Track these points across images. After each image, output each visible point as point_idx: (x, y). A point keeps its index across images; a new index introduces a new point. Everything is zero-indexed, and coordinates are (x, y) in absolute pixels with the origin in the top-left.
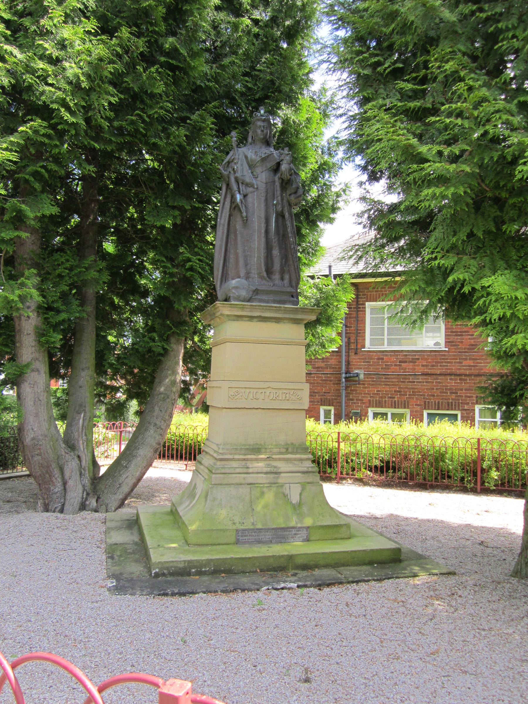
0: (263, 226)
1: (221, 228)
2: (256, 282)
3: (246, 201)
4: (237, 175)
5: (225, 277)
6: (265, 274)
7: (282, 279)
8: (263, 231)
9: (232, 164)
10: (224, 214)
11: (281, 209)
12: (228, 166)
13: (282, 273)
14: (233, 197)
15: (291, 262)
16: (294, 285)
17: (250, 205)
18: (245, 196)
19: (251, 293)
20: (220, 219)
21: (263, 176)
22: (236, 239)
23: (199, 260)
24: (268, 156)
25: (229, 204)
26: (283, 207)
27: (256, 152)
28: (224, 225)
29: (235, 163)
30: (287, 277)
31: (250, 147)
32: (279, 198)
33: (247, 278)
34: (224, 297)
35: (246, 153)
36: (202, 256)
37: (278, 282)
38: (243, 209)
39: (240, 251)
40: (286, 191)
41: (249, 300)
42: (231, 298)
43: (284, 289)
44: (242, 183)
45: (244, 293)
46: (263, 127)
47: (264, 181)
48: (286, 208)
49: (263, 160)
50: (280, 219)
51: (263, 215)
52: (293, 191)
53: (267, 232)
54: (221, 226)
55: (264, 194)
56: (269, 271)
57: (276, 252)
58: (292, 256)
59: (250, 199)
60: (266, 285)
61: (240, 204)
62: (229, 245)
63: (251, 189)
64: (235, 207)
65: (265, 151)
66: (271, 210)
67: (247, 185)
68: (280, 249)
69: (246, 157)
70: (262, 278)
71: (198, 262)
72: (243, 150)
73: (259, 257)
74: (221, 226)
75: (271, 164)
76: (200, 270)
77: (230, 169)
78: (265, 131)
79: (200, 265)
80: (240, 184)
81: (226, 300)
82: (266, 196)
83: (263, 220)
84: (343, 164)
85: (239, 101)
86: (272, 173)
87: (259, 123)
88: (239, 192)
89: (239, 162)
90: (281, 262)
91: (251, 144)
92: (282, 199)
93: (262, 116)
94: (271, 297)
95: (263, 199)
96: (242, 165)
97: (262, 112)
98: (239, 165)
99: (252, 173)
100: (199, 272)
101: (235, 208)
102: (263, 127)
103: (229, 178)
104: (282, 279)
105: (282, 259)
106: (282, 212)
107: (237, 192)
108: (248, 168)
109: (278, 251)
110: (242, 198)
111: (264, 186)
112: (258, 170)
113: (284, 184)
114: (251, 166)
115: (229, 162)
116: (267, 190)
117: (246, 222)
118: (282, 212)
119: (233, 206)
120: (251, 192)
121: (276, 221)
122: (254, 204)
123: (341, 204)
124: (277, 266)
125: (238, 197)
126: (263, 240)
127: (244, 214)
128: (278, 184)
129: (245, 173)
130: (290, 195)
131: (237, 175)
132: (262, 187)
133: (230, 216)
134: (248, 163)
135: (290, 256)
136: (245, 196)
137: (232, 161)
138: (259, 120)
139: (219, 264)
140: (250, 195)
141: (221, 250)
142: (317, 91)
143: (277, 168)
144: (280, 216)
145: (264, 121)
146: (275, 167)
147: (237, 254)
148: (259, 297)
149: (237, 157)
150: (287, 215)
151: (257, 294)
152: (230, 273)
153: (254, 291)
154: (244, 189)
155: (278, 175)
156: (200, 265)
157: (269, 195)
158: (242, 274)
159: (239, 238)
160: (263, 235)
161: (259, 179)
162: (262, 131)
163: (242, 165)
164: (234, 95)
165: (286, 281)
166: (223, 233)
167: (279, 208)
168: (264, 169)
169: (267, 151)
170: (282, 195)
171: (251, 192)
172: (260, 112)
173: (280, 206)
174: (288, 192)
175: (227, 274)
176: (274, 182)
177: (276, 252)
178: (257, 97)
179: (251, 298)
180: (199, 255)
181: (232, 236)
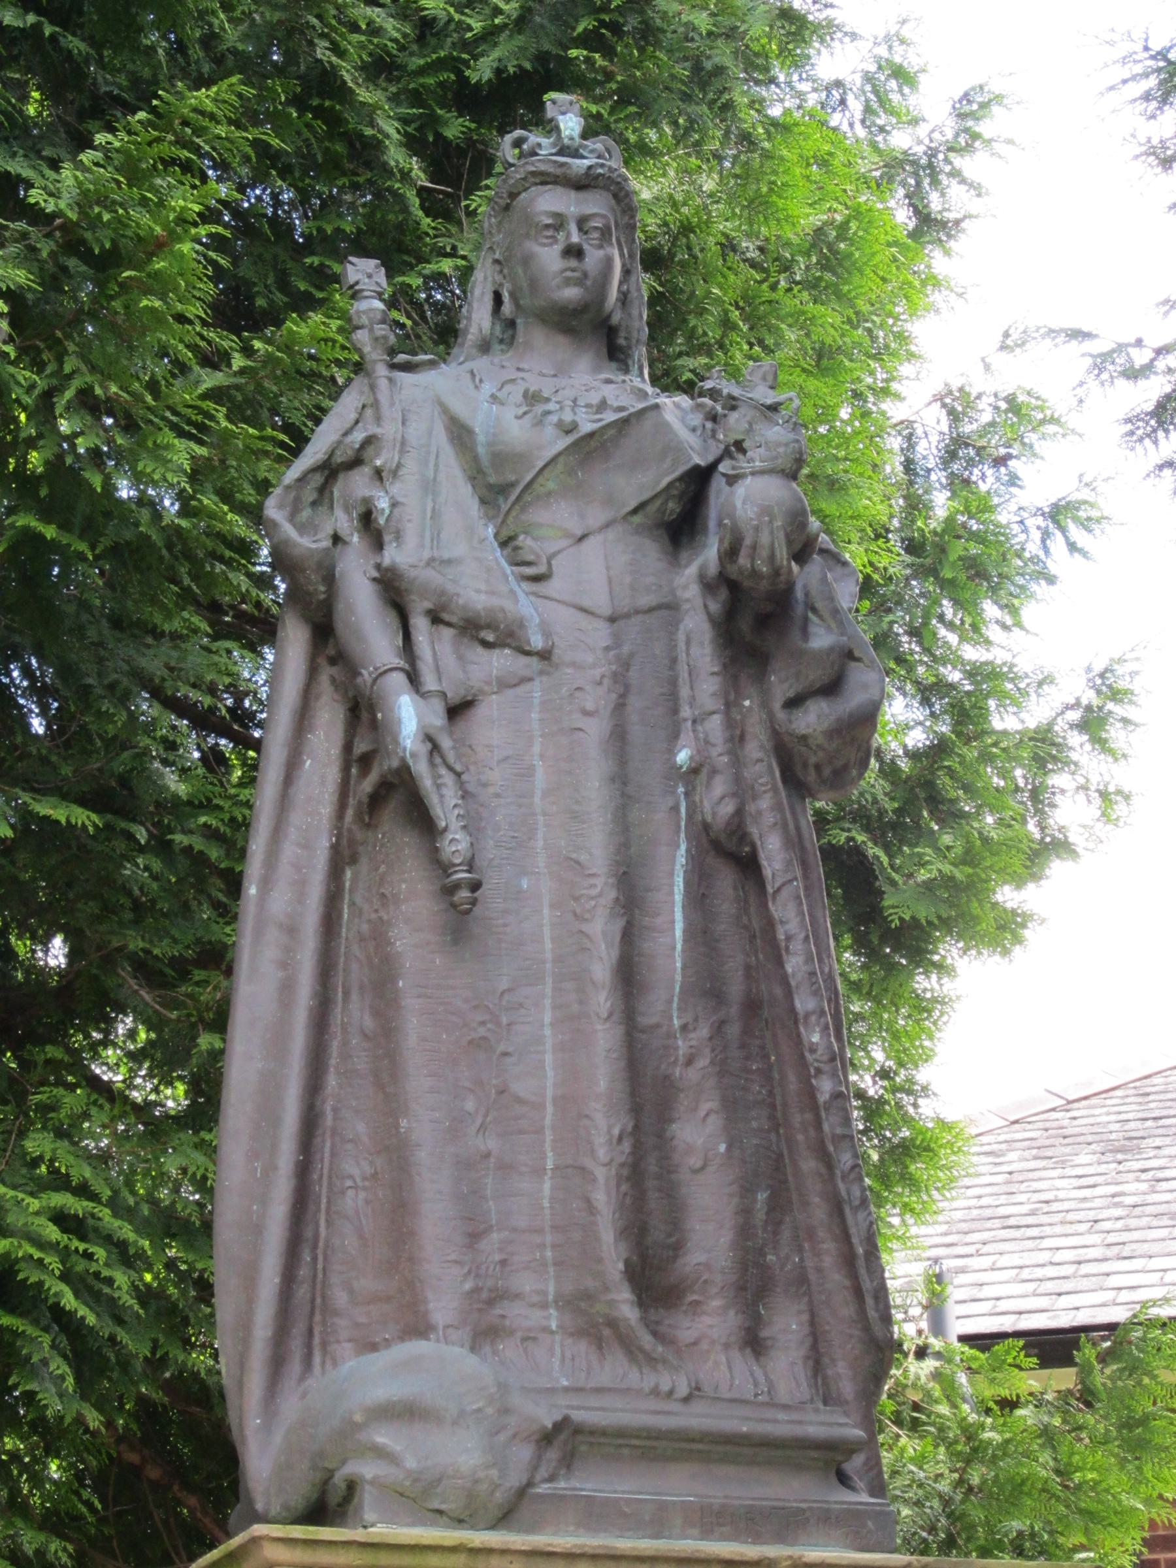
0: (602, 931)
1: (271, 953)
2: (557, 1374)
3: (460, 743)
4: (392, 555)
5: (301, 1327)
6: (627, 1309)
7: (754, 1342)
8: (602, 969)
9: (358, 484)
10: (289, 851)
11: (728, 808)
12: (324, 490)
13: (753, 1288)
14: (363, 712)
15: (819, 1211)
16: (847, 1388)
17: (496, 776)
18: (457, 710)
19: (524, 1453)
20: (266, 884)
21: (592, 565)
22: (386, 1036)
23: (61, 1219)
24: (624, 424)
25: (333, 774)
26: (742, 792)
27: (533, 398)
28: (291, 930)
29: (378, 473)
30: (787, 1325)
31: (481, 364)
32: (715, 726)
33: (485, 1334)
34: (299, 1494)
35: (459, 408)
36: (83, 1191)
37: (728, 1371)
38: (445, 805)
39: (423, 1125)
40: (760, 677)
41: (504, 1518)
42: (367, 1498)
43: (781, 1426)
44: (436, 619)
45: (461, 1453)
46: (582, 222)
47: (601, 601)
48: (765, 803)
49: (590, 449)
50: (726, 880)
51: (597, 850)
52: (816, 675)
53: (629, 975)
54: (273, 935)
55: (597, 698)
56: (656, 1281)
57: (699, 1134)
58: (828, 1162)
59: (489, 728)
60: (620, 1395)
61: (421, 768)
62: (332, 1081)
63: (501, 661)
64: (386, 797)
65: (590, 391)
66: (660, 816)
67: (478, 630)
68: (732, 1107)
69: (460, 434)
70: (599, 1331)
71: (53, 1233)
72: (442, 384)
73: (574, 1172)
74: (273, 935)
75: (642, 481)
76: (69, 1301)
77: (343, 521)
78: (593, 257)
79: (65, 1254)
80: (420, 625)
81: (319, 1511)
82: (620, 707)
83: (601, 888)
84: (1057, 543)
85: (365, 95)
86: (652, 552)
87: (549, 202)
88: (414, 679)
89: (411, 466)
90: (745, 1212)
91: (485, 347)
92: (737, 738)
93: (563, 151)
94: (681, 1486)
95: (596, 730)
96: (429, 487)
97: (570, 125)
98: (405, 488)
99: (506, 542)
100: (60, 1315)
101: (376, 801)
102: (582, 222)
103: (330, 578)
104: (754, 1342)
105: (746, 1190)
106: (738, 827)
107: (398, 680)
108: (473, 506)
109: (715, 1123)
110: (437, 719)
111: (600, 634)
112: (553, 521)
113: (745, 624)
114: (501, 488)
115: (330, 471)
116: (625, 664)
117: (460, 900)
118: (738, 827)
119: (368, 785)
120: (504, 684)
121: (699, 897)
122: (528, 773)
123: (1070, 812)
124: (709, 1242)
125: (409, 717)
126: (605, 1039)
127: (455, 844)
128: (696, 625)
129: (457, 549)
130: (794, 703)
131: (392, 555)
132: (586, 646)
133: (341, 859)
134: (475, 474)
135: (809, 1165)
136: (457, 710)
137: (356, 462)
138: (546, 179)
139: (257, 1230)
140: (489, 709)
141: (275, 1122)
142: (855, 80)
143: (682, 513)
144: (729, 852)
145: (583, 184)
146: (673, 507)
147: (396, 1154)
148: (588, 1483)
149: (389, 430)
150: (773, 854)
151: (568, 1461)
152: (340, 1298)
153: (547, 1438)
154: (449, 659)
155: (709, 554)
156: (65, 1254)
157: (635, 703)
158: (443, 1307)
159: (414, 1027)
160: (603, 1000)
161: (554, 587)
162: (574, 252)
163: (429, 487)
164: (322, 51)
165: (786, 1366)
166: (287, 987)
167: (716, 801)
168: (597, 516)
169: (609, 392)
170: (730, 705)
171: (504, 684)
172: (551, 128)
173: (720, 786)
174: (781, 687)
175: (320, 1305)
176: (670, 608)
177: (699, 1134)
178: (482, 71)
179: (522, 1492)
180: (59, 1181)
181: (354, 1014)
